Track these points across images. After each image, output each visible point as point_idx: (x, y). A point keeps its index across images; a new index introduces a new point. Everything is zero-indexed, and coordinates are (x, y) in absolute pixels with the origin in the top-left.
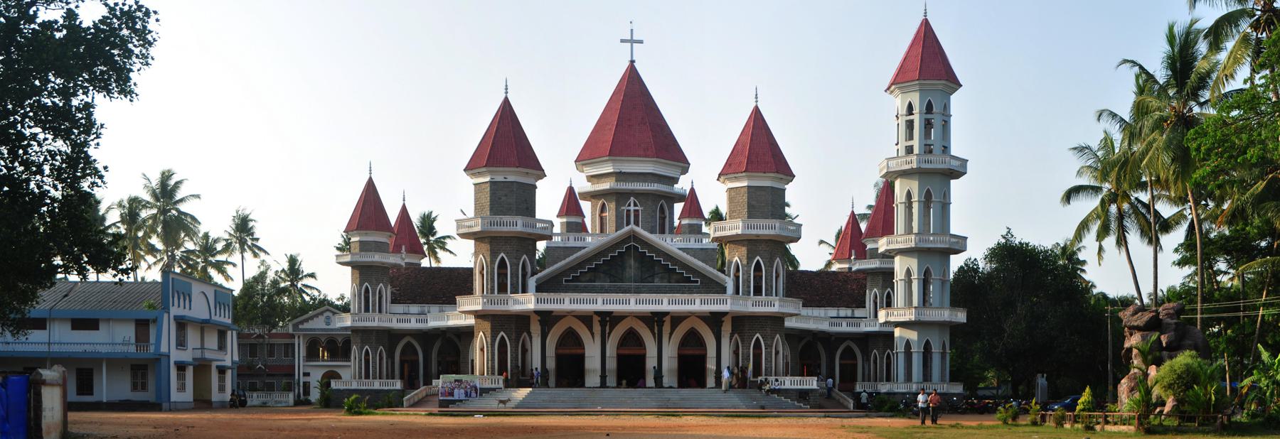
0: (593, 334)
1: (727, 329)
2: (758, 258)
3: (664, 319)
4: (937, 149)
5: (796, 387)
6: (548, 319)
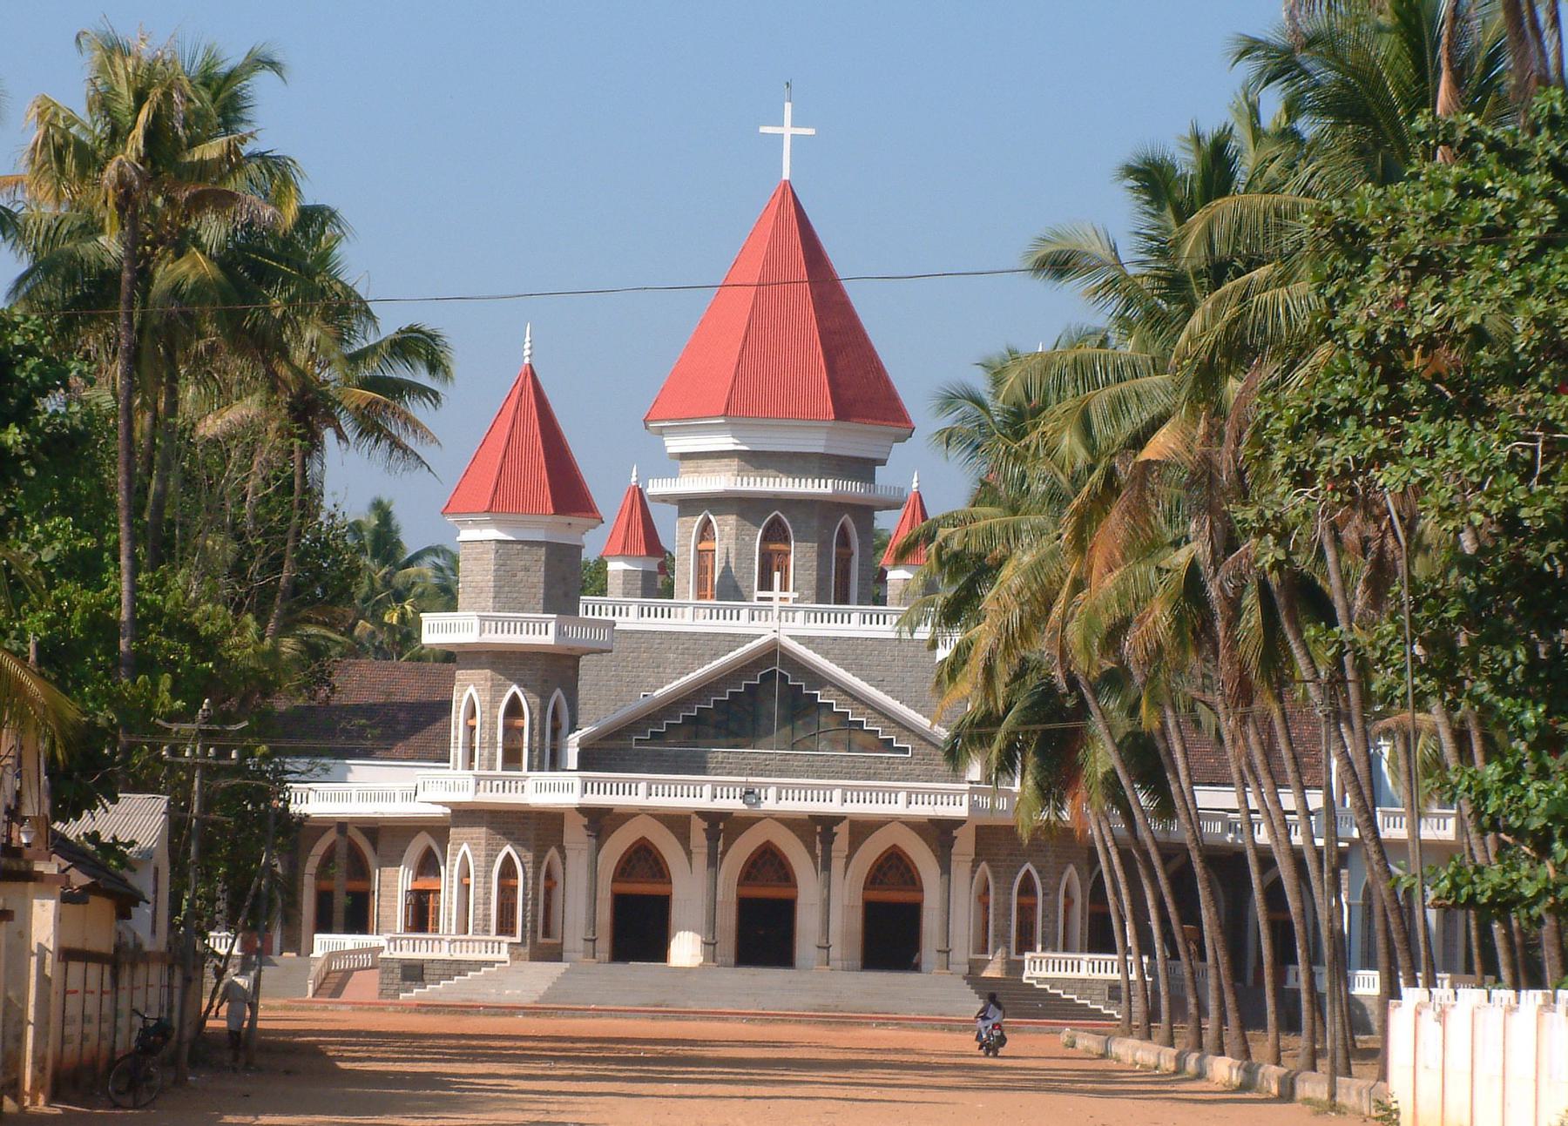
0: (689, 853)
6: (600, 821)
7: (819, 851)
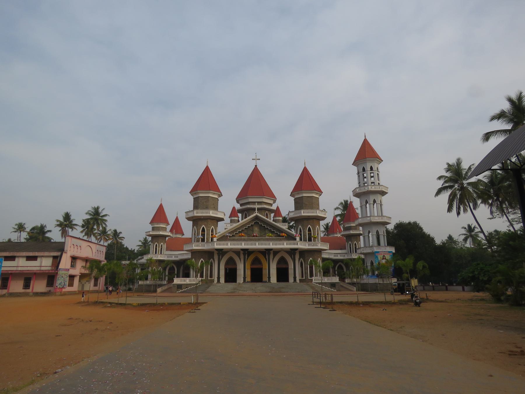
0: (240, 259)
1: (297, 257)
2: (309, 226)
3: (271, 252)
4: (377, 183)
5: (329, 281)
6: (221, 252)
7: (267, 258)
